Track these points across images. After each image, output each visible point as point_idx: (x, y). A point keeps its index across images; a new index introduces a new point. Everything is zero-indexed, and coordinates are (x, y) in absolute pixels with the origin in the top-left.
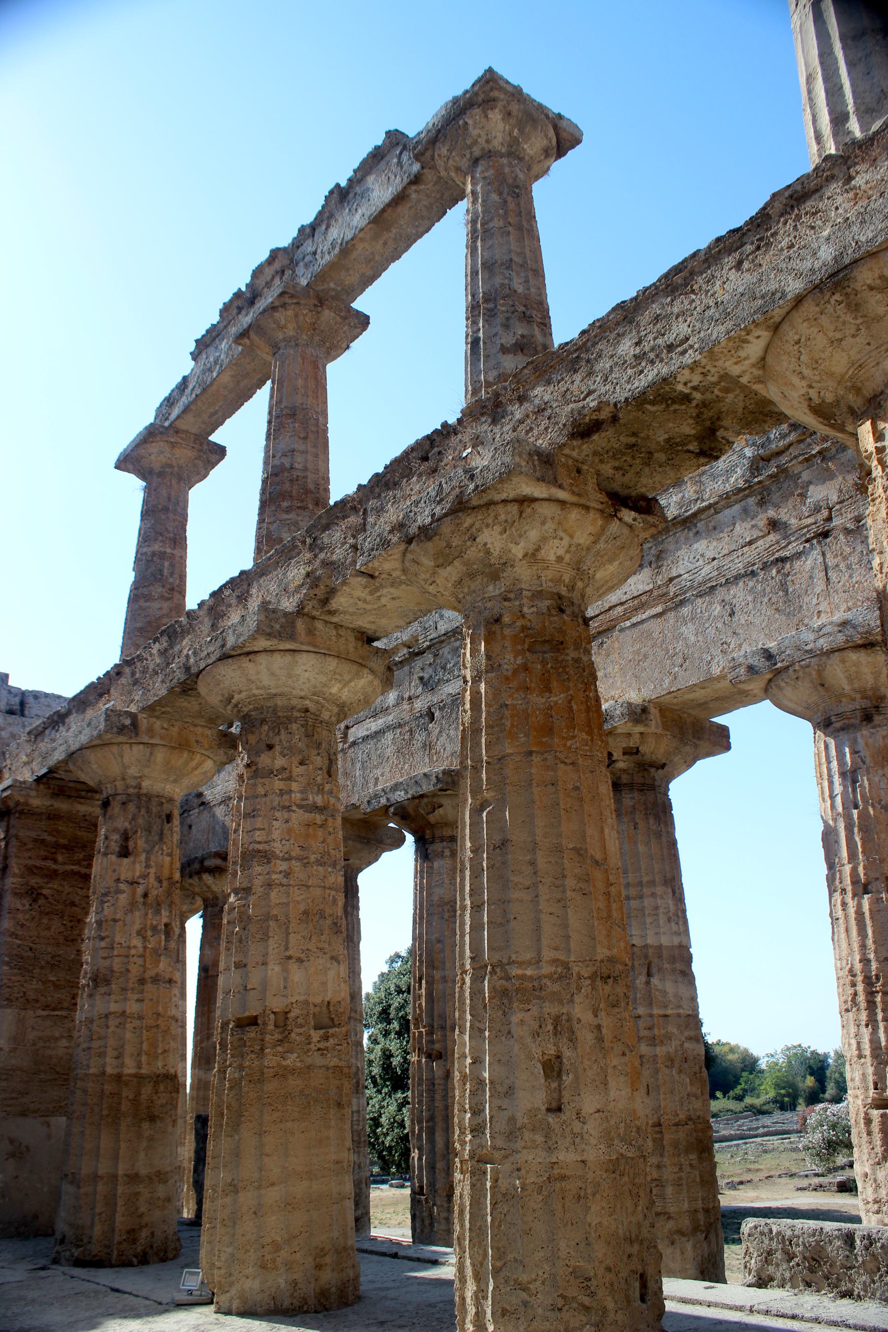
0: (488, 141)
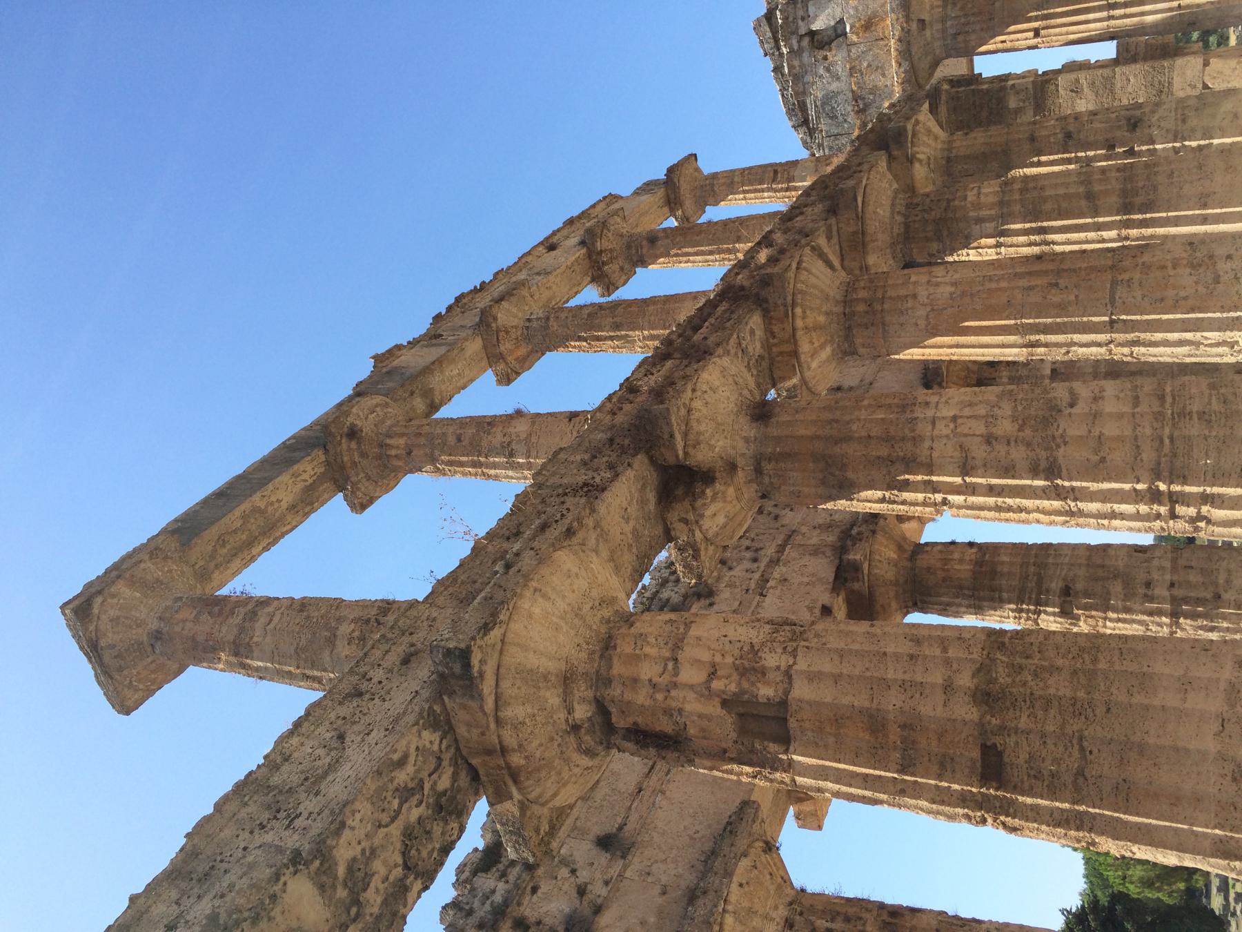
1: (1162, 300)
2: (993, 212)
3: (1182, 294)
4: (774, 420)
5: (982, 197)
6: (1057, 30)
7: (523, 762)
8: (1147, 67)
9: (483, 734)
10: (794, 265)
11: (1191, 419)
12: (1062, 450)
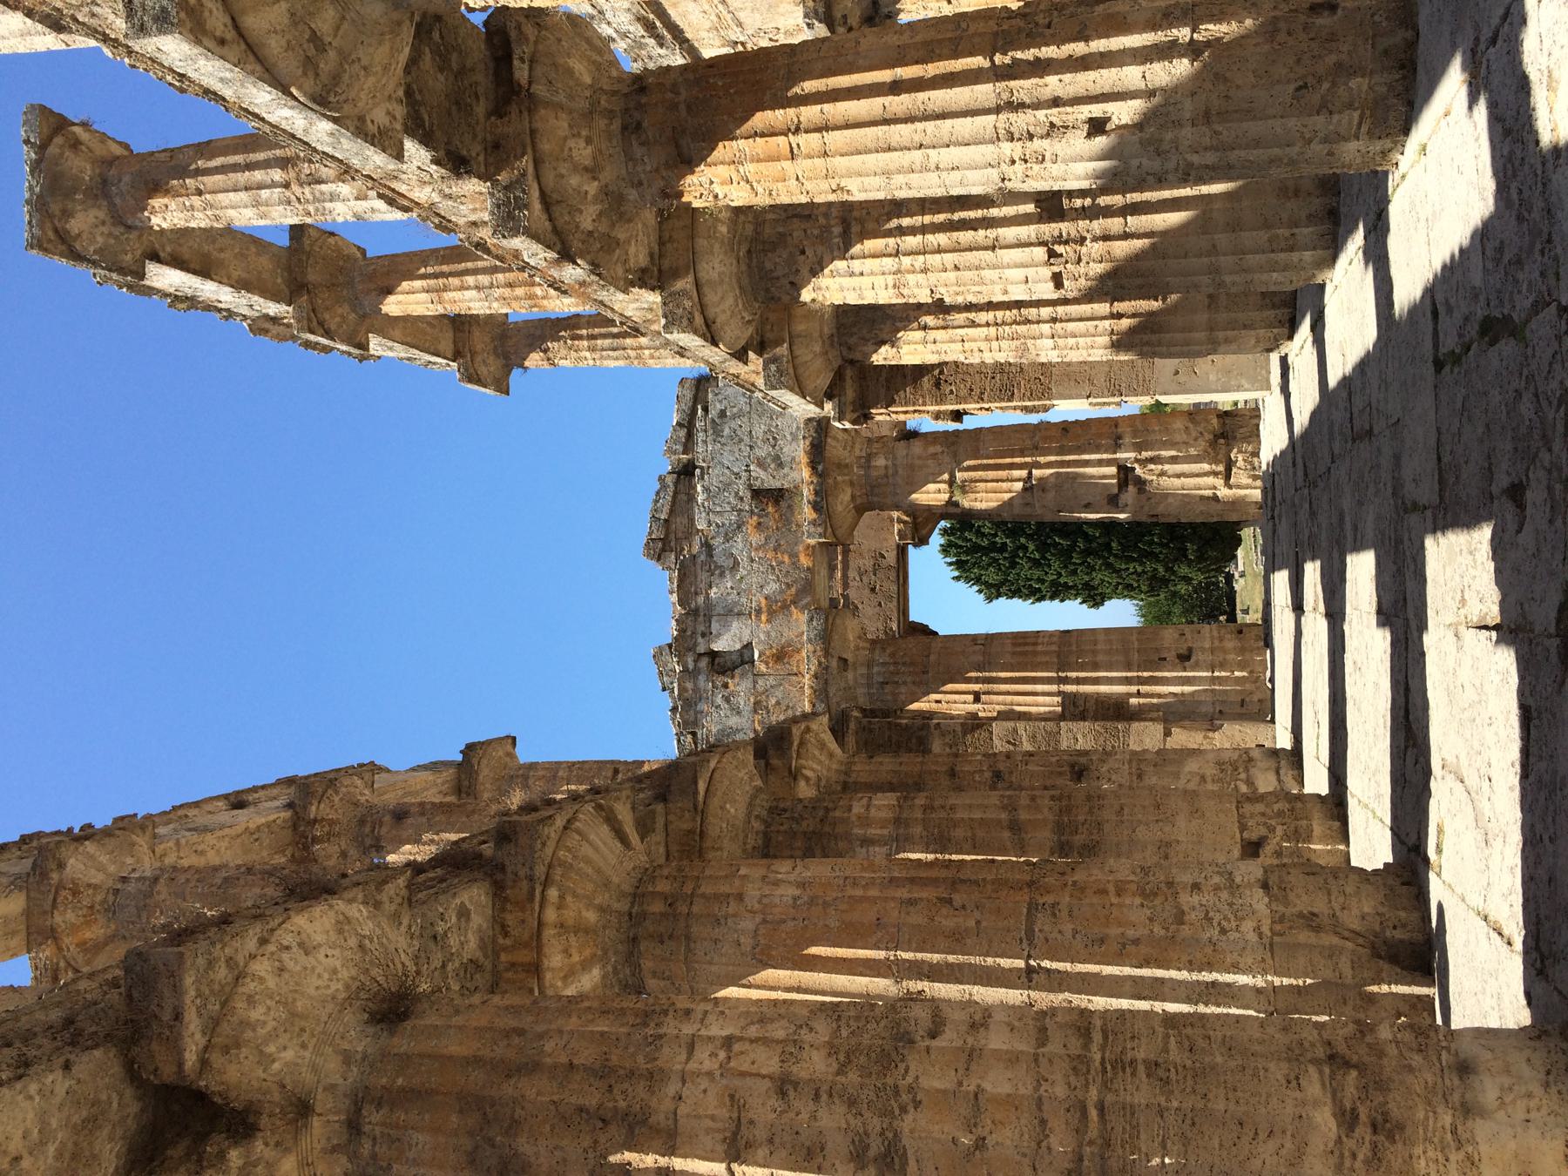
0: (103, 223)
1: (1102, 941)
2: (885, 832)
3: (1131, 933)
4: (408, 1024)
5: (873, 811)
6: (1001, 698)
8: (1098, 726)
10: (560, 822)
11: (1133, 1074)
12: (909, 1118)
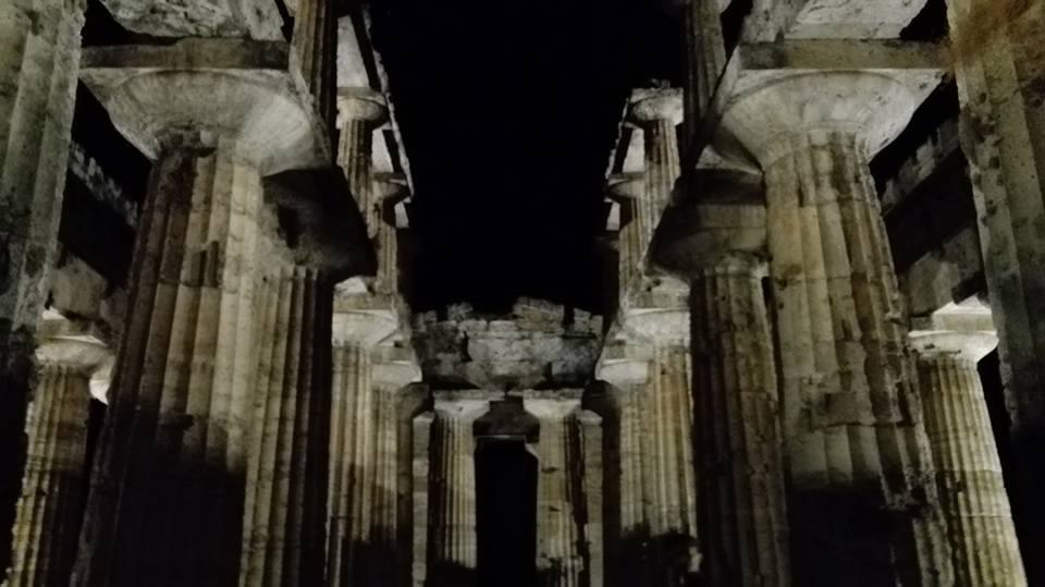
7: (178, 83)
9: (208, 60)
